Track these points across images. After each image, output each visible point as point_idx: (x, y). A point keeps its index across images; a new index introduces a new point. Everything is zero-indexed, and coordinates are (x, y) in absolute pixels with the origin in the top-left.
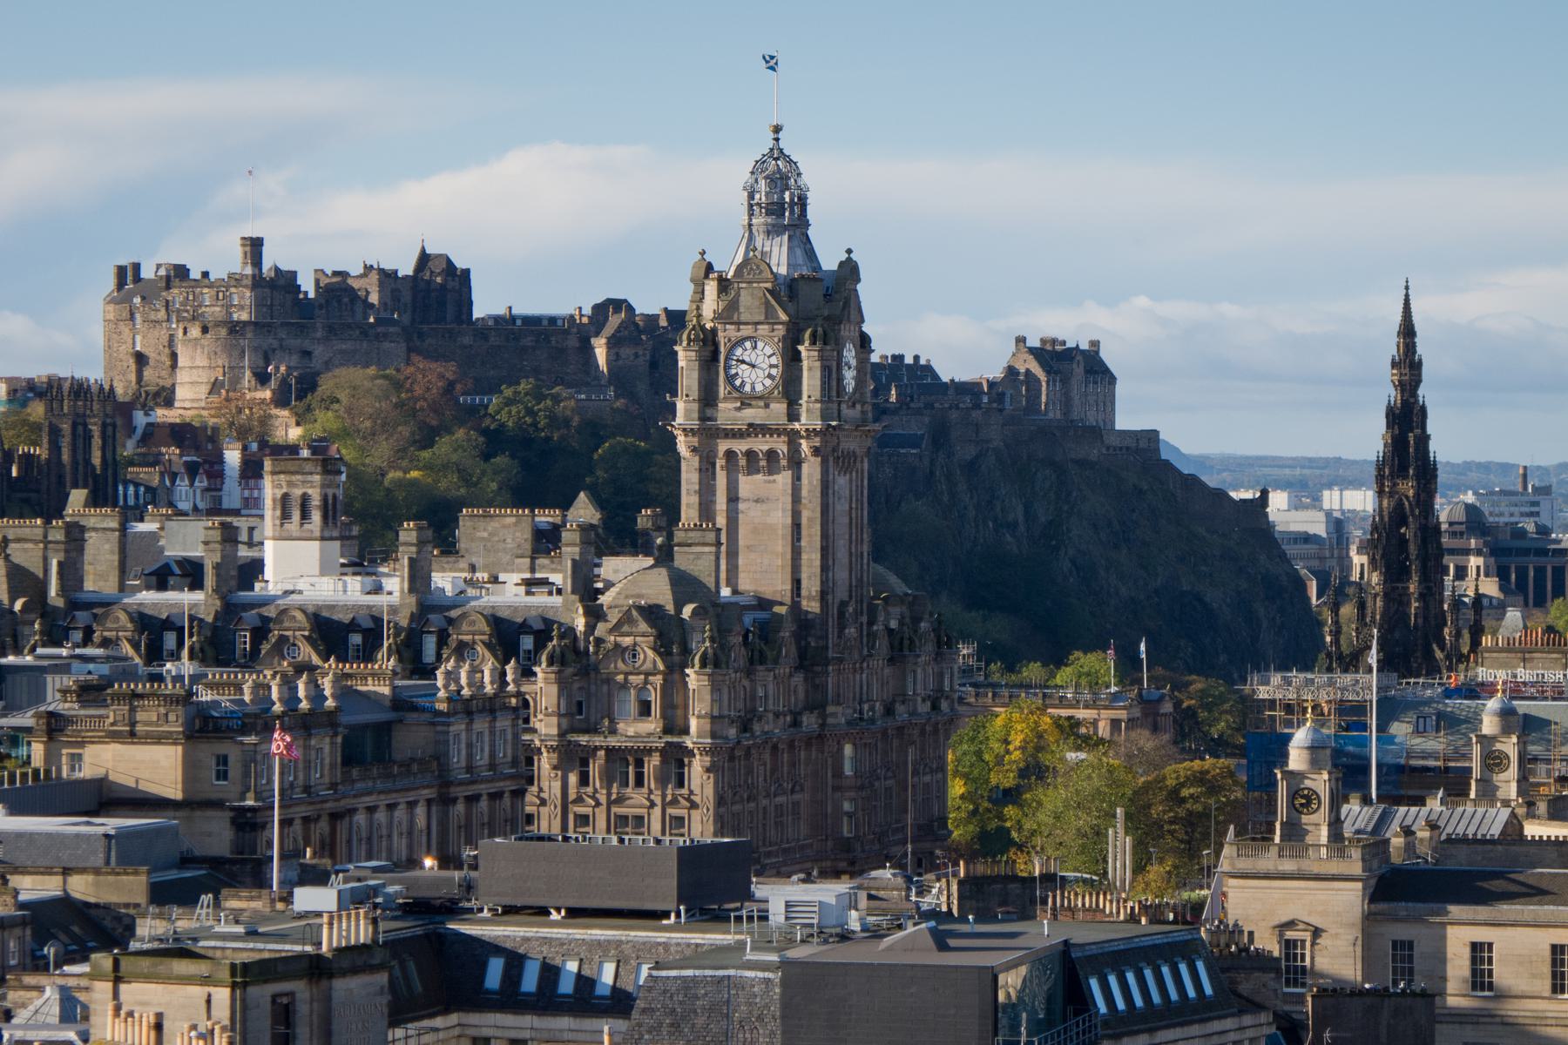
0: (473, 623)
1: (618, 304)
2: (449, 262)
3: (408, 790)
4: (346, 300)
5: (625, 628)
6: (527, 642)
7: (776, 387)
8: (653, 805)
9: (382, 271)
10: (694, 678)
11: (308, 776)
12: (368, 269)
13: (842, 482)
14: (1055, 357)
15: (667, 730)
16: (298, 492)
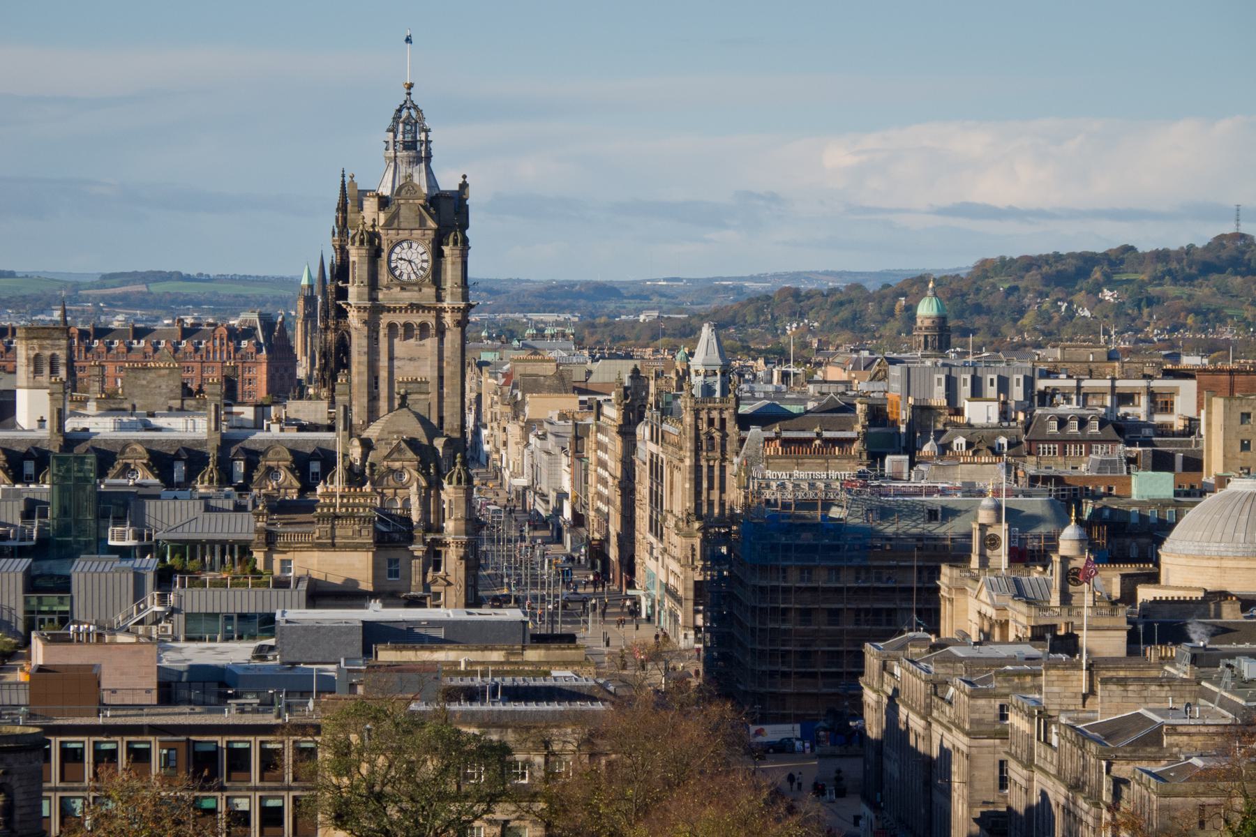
0: (278, 453)
5: (395, 456)
7: (427, 276)
16: (48, 353)
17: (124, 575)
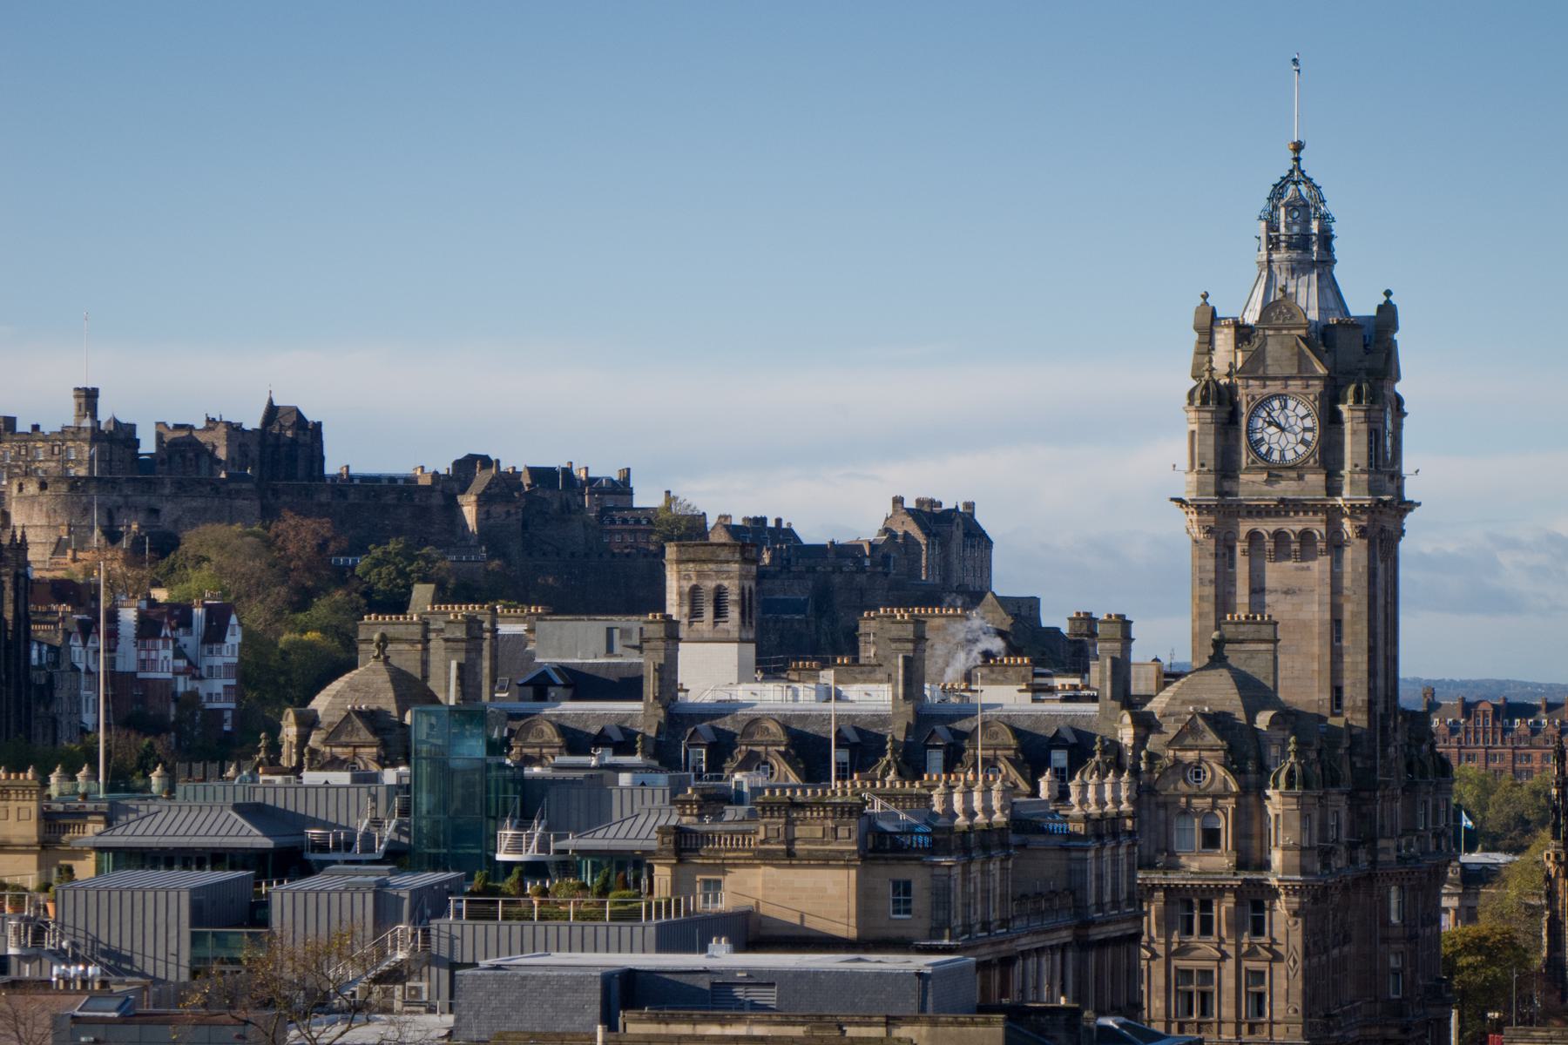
0: (995, 735)
1: (486, 462)
2: (300, 415)
3: (1053, 930)
4: (190, 455)
5: (1189, 741)
6: (1060, 758)
7: (1312, 454)
8: (1224, 956)
9: (229, 424)
10: (1276, 802)
11: (986, 912)
12: (212, 423)
13: (1381, 567)
14: (931, 517)
15: (1241, 865)
16: (710, 584)
17: (358, 897)
